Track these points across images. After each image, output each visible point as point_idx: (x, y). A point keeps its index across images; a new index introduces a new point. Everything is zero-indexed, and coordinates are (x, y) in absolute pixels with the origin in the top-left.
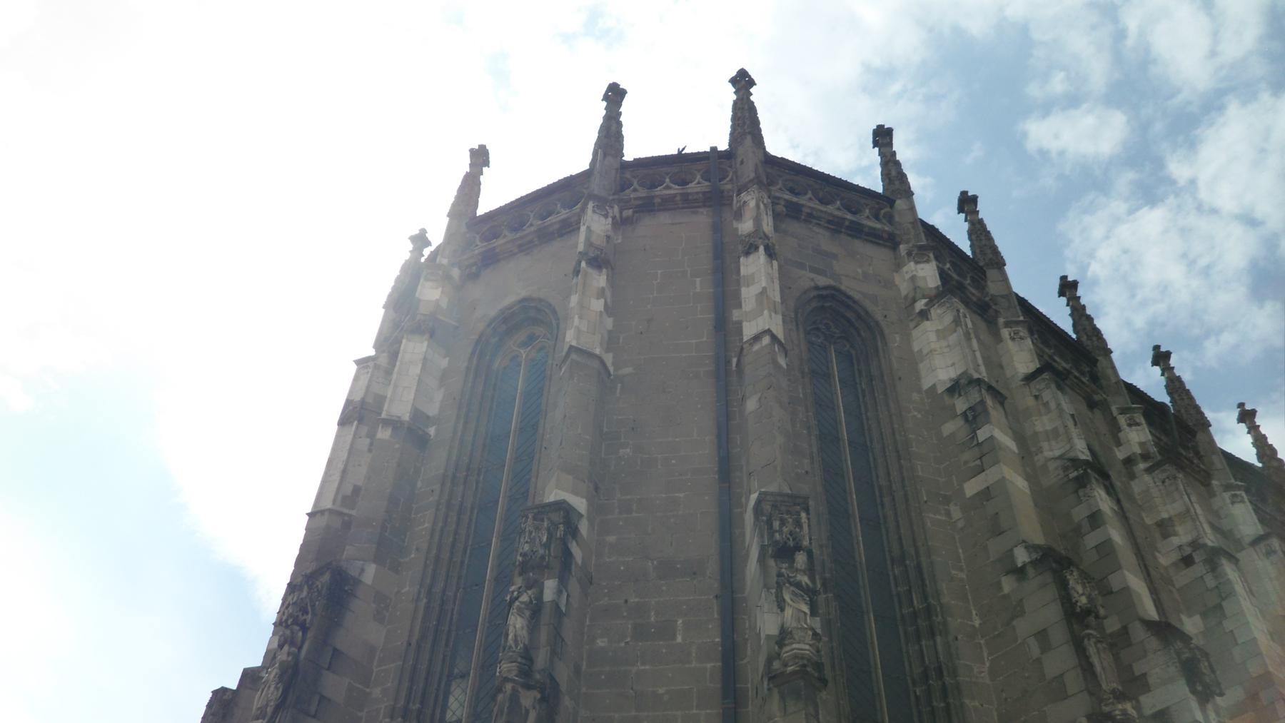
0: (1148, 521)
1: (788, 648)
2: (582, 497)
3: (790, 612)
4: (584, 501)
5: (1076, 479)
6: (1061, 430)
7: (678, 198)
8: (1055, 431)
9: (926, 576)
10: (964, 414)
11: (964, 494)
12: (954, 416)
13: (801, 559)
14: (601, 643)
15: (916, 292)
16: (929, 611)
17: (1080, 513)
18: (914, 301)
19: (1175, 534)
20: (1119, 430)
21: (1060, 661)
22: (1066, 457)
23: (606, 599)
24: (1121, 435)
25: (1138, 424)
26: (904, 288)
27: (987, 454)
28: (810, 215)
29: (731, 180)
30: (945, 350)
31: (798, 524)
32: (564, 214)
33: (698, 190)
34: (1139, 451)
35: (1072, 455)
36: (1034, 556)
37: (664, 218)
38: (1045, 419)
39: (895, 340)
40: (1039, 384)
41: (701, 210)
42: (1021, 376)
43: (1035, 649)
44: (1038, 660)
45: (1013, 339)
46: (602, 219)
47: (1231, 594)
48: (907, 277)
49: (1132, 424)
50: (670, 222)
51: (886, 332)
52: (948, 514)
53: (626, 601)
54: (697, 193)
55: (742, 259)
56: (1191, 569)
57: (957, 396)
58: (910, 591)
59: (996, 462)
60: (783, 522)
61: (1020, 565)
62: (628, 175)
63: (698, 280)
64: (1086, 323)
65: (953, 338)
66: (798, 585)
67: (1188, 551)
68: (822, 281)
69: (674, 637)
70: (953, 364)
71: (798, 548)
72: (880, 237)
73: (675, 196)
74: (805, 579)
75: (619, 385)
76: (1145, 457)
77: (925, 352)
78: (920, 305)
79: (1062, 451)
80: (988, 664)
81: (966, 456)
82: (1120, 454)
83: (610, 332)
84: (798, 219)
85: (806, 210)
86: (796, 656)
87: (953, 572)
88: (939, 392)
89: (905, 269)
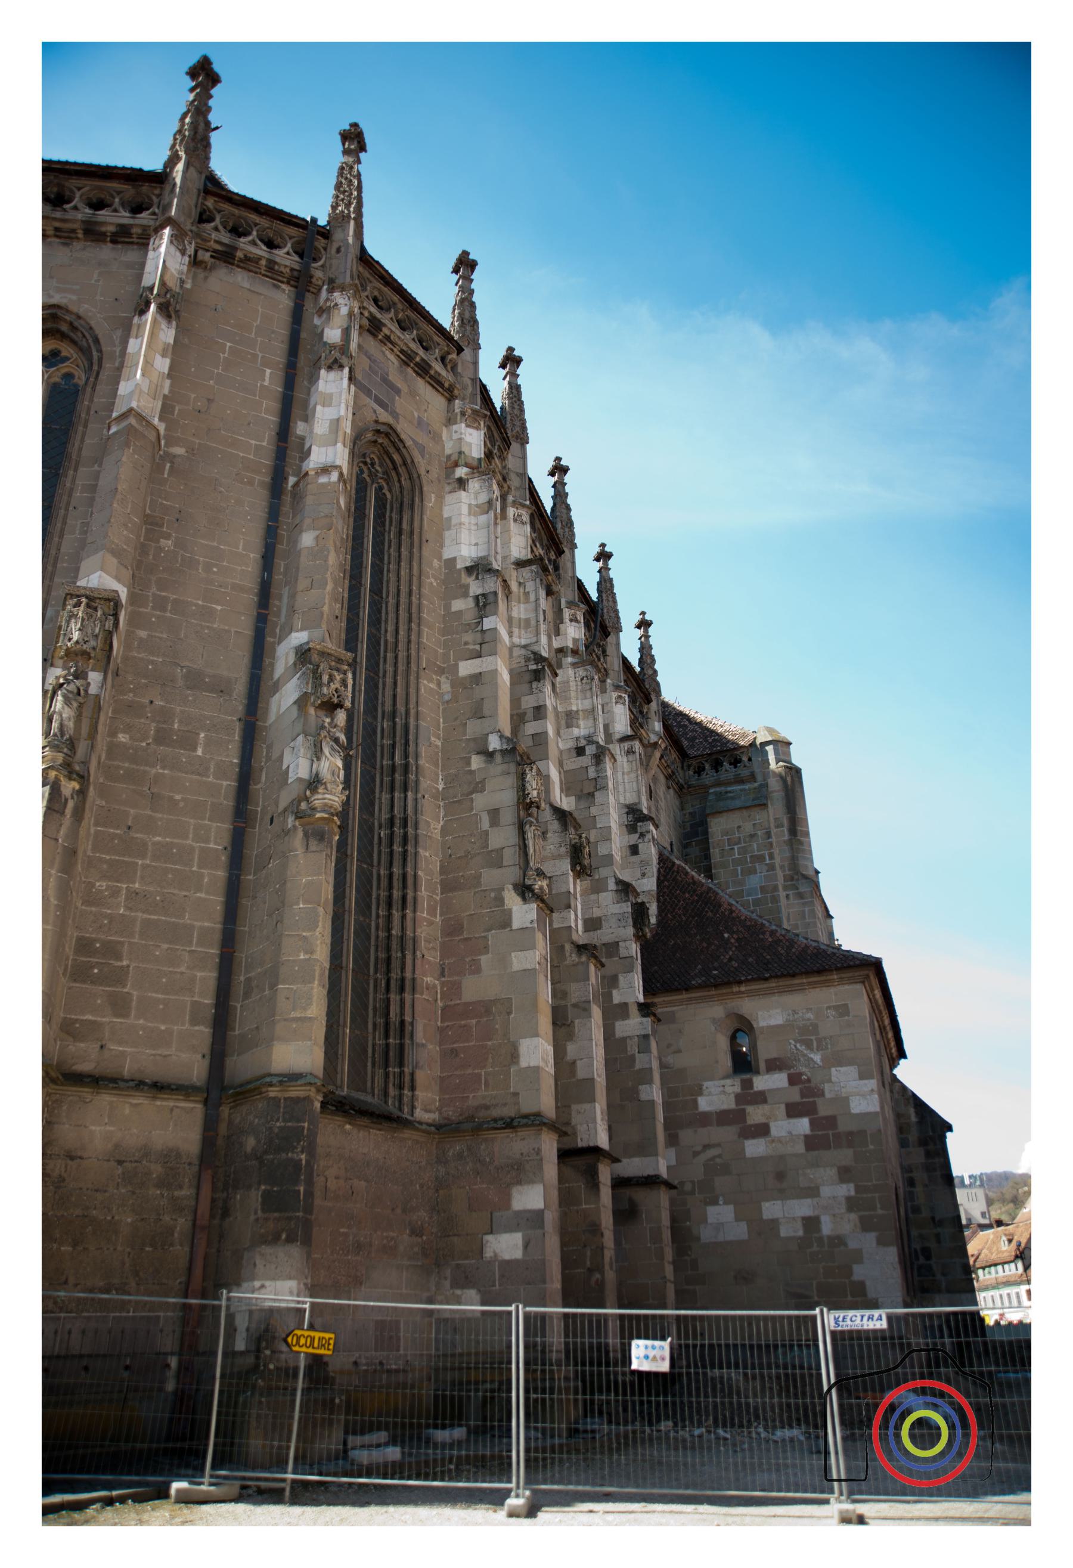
1: (320, 796)
2: (124, 585)
3: (327, 764)
4: (125, 590)
5: (535, 671)
6: (533, 623)
7: (263, 262)
8: (527, 621)
9: (411, 737)
10: (476, 598)
11: (458, 672)
12: (465, 594)
13: (341, 717)
14: (122, 738)
15: (459, 457)
16: (406, 767)
18: (456, 465)
19: (578, 727)
21: (503, 837)
22: (531, 648)
23: (131, 695)
25: (577, 621)
26: (449, 448)
27: (486, 644)
28: (388, 338)
29: (323, 266)
30: (473, 528)
31: (344, 683)
32: (124, 217)
33: (288, 263)
35: (535, 648)
36: (505, 747)
37: (241, 278)
38: (522, 605)
39: (431, 500)
40: (526, 572)
41: (283, 286)
42: (513, 560)
43: (485, 824)
44: (486, 833)
45: (515, 520)
46: (178, 254)
47: (605, 788)
48: (455, 436)
49: (574, 619)
50: (247, 285)
51: (425, 489)
52: (439, 684)
53: (151, 702)
54: (286, 266)
55: (323, 372)
56: (580, 758)
57: (474, 577)
58: (393, 746)
59: (494, 653)
60: (331, 679)
61: (491, 750)
63: (268, 371)
64: (565, 511)
65: (483, 519)
66: (336, 740)
67: (583, 743)
68: (384, 416)
69: (195, 749)
70: (476, 544)
71: (340, 706)
72: (442, 385)
73: (260, 258)
74: (342, 737)
75: (168, 465)
76: (575, 652)
77: (454, 522)
78: (461, 472)
79: (528, 641)
80: (442, 823)
81: (468, 637)
83: (165, 396)
84: (375, 336)
85: (385, 331)
86: (326, 805)
87: (433, 739)
88: (459, 566)
89: (455, 427)
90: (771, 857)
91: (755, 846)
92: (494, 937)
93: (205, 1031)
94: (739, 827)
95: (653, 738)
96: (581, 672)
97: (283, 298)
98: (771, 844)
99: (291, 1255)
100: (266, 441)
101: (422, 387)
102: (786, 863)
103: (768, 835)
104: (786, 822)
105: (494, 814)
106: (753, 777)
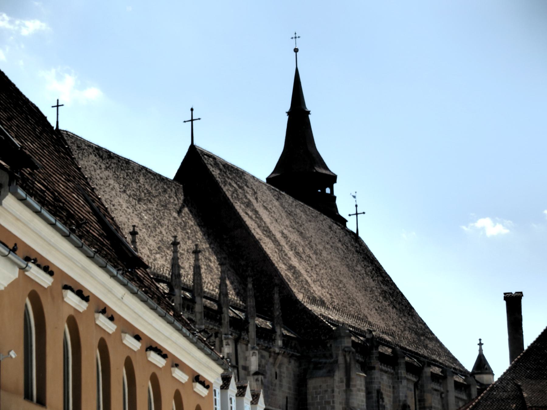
20: (222, 346)
24: (222, 348)
49: (228, 344)
90: (333, 402)
91: (327, 396)
94: (320, 386)
95: (277, 350)
98: (333, 396)
102: (344, 402)
103: (333, 391)
104: (345, 380)
106: (331, 356)
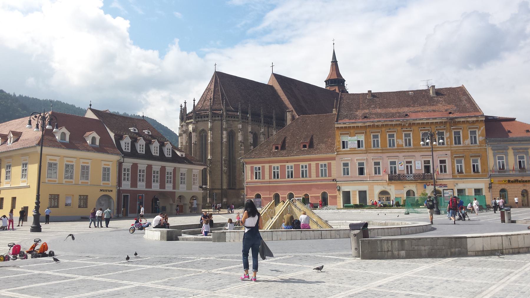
0: (261, 140)
17: (250, 148)
34: (262, 132)
37: (216, 122)
39: (237, 134)
40: (251, 133)
62: (213, 115)
68: (231, 129)
78: (239, 130)
82: (261, 132)
92: (242, 175)
93: (221, 185)
96: (263, 135)
97: (220, 122)
99: (225, 198)
100: (220, 139)
101: (235, 122)
105: (241, 165)
